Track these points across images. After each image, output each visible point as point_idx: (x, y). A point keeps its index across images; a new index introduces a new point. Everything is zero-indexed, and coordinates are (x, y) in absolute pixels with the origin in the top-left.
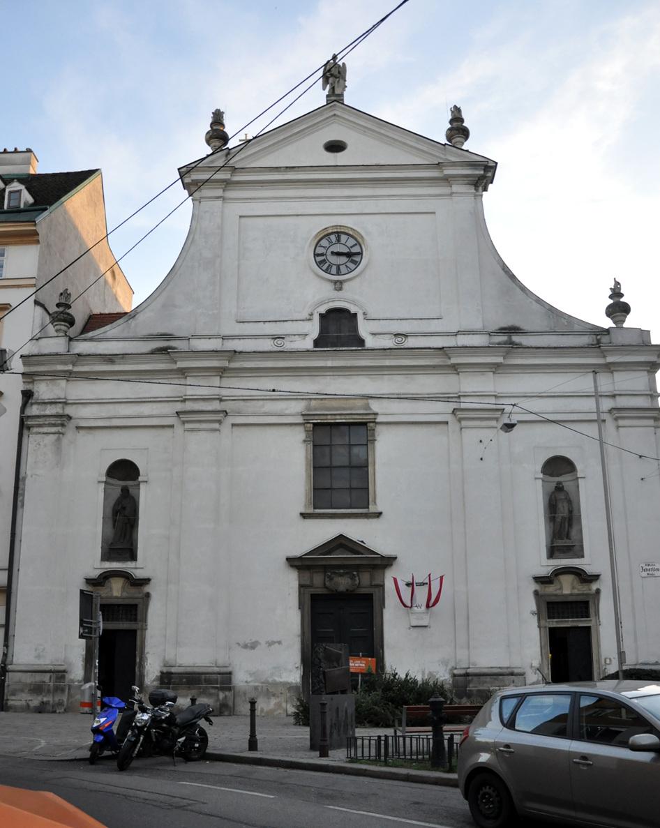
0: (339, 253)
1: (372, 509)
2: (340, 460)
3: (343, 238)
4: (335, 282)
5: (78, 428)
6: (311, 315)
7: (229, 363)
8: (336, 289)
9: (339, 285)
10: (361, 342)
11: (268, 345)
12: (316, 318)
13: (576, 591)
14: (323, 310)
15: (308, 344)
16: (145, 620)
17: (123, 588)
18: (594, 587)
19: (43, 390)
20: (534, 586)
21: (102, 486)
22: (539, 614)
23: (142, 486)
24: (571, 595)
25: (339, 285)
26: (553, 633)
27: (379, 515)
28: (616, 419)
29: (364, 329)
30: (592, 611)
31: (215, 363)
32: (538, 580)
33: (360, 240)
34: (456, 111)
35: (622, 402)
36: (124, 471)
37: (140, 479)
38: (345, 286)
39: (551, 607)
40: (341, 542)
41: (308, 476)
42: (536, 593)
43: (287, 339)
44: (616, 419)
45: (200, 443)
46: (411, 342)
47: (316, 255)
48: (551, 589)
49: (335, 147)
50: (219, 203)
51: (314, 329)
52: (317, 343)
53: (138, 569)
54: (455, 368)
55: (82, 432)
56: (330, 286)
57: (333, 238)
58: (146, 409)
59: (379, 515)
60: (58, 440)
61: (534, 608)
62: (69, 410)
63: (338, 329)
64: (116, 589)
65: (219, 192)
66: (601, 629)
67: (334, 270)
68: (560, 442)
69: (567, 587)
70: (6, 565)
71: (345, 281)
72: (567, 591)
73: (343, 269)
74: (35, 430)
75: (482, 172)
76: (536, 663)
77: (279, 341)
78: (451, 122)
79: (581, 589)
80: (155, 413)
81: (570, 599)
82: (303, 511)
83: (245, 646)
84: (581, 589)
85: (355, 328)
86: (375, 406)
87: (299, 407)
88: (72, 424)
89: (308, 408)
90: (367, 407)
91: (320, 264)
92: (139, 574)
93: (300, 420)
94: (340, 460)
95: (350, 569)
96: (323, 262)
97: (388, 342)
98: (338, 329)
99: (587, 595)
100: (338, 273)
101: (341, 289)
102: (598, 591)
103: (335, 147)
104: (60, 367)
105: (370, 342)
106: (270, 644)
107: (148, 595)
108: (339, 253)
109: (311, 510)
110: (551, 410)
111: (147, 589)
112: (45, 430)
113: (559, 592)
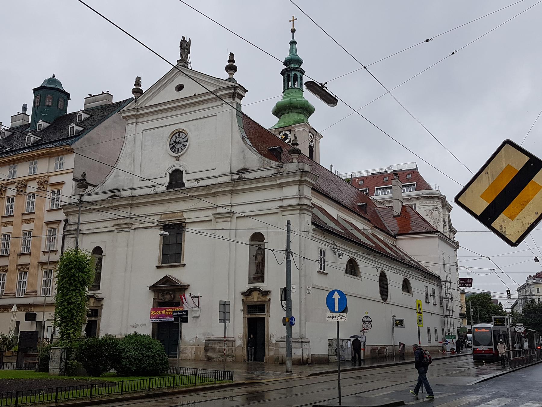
0: (178, 143)
1: (182, 263)
3: (181, 134)
4: (176, 157)
5: (83, 234)
7: (133, 202)
8: (177, 160)
9: (177, 158)
10: (184, 185)
11: (149, 191)
12: (168, 175)
13: (260, 300)
14: (170, 171)
15: (164, 189)
17: (94, 303)
19: (73, 219)
20: (242, 297)
22: (243, 310)
24: (258, 301)
25: (177, 158)
27: (184, 265)
29: (185, 178)
30: (266, 309)
31: (126, 202)
32: (242, 293)
34: (232, 55)
37: (103, 254)
38: (180, 158)
39: (250, 308)
40: (166, 280)
41: (160, 249)
42: (243, 300)
43: (157, 187)
45: (122, 237)
46: (202, 183)
47: (170, 145)
48: (249, 299)
49: (180, 88)
50: (134, 125)
51: (166, 181)
52: (168, 187)
54: (215, 194)
55: (85, 236)
56: (175, 159)
57: (177, 135)
59: (184, 265)
63: (176, 179)
65: (134, 120)
66: (270, 319)
67: (176, 152)
68: (256, 225)
69: (255, 298)
71: (180, 156)
72: (256, 300)
73: (180, 150)
74: (68, 236)
75: (233, 91)
76: (241, 336)
77: (152, 189)
78: (229, 61)
79: (262, 298)
80: (108, 225)
81: (258, 303)
82: (157, 265)
84: (262, 298)
86: (185, 216)
88: (81, 232)
89: (161, 219)
91: (171, 149)
92: (100, 296)
95: (174, 291)
96: (173, 147)
97: (193, 184)
98: (176, 179)
99: (265, 301)
100: (178, 152)
101: (179, 160)
102: (270, 300)
103: (180, 88)
104: (75, 209)
105: (187, 185)
106: (142, 325)
107: (102, 305)
108: (178, 143)
109: (160, 265)
110: (254, 209)
112: (71, 236)
113: (252, 300)
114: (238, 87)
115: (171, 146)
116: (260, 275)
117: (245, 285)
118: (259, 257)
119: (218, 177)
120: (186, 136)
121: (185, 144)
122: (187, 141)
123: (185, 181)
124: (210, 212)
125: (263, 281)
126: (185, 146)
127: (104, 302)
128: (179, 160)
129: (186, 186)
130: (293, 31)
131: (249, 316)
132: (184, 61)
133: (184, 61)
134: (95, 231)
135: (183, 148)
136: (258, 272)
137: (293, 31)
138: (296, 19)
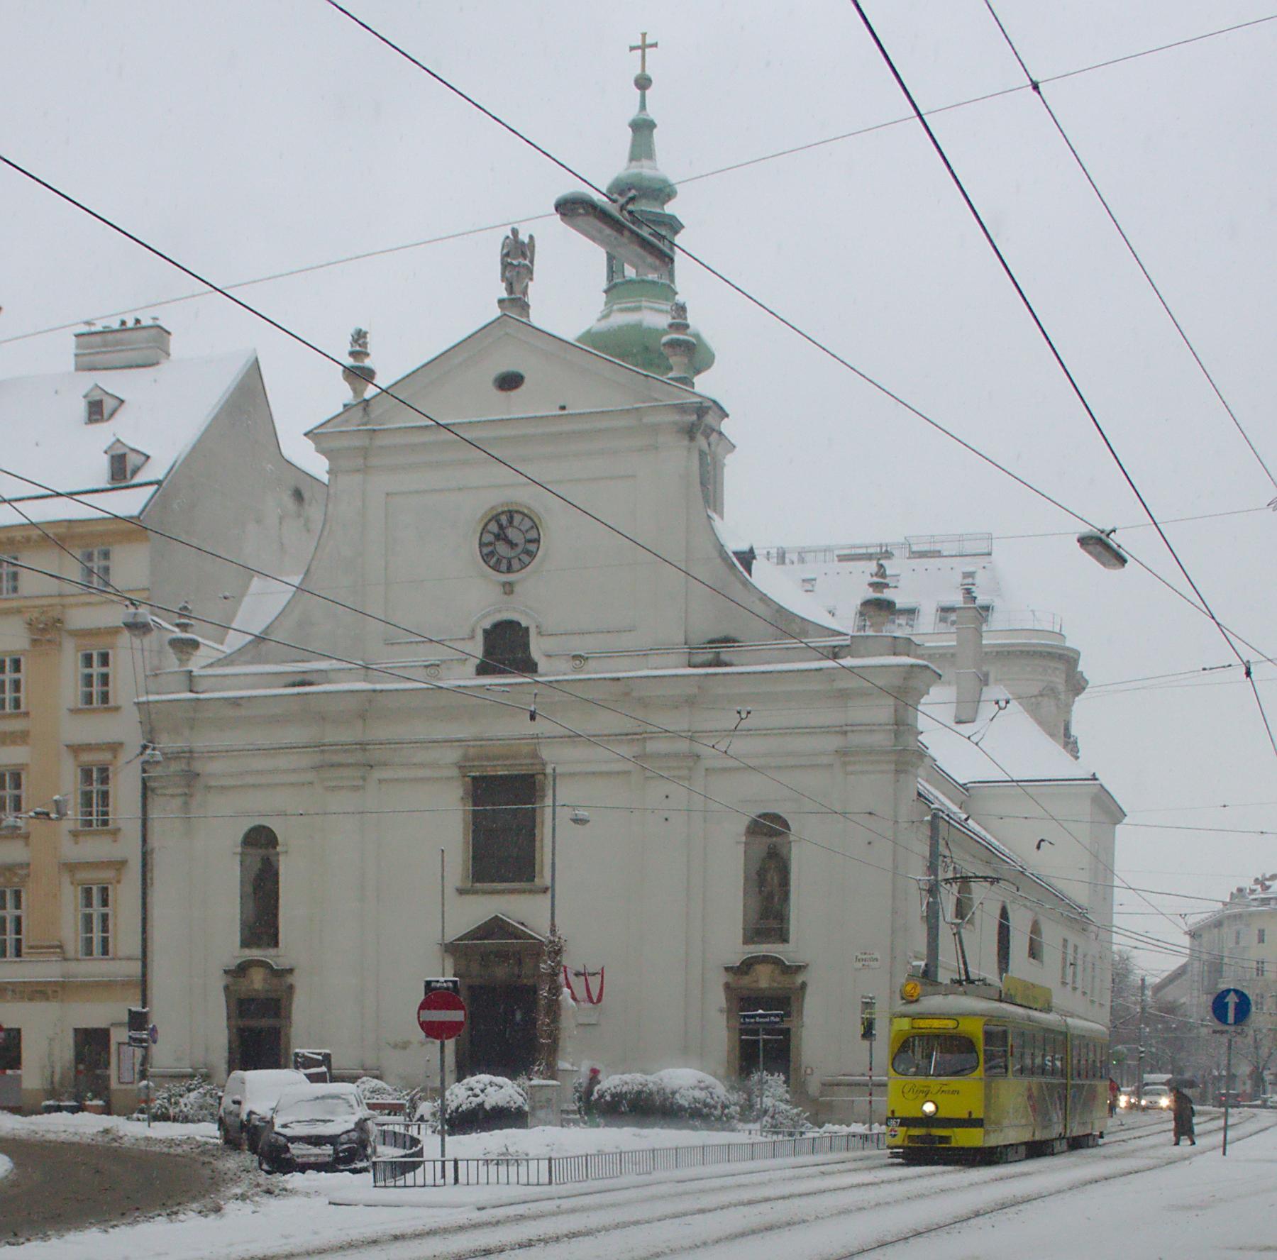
0: (507, 540)
2: (505, 821)
3: (517, 518)
6: (473, 631)
9: (508, 588)
10: (529, 666)
14: (487, 624)
16: (289, 1017)
17: (265, 980)
18: (799, 979)
21: (238, 858)
23: (282, 858)
25: (508, 588)
26: (241, 1031)
28: (845, 764)
32: (727, 969)
33: (536, 520)
35: (855, 740)
36: (261, 841)
37: (279, 849)
38: (517, 588)
40: (496, 927)
42: (727, 986)
44: (845, 764)
47: (481, 545)
48: (746, 981)
49: (509, 382)
51: (477, 648)
52: (482, 670)
53: (277, 957)
56: (500, 590)
57: (504, 519)
58: (283, 762)
60: (186, 803)
61: (724, 1004)
62: (198, 766)
63: (506, 648)
64: (257, 980)
66: (805, 1033)
67: (504, 566)
69: (764, 979)
70: (138, 952)
72: (764, 984)
82: (459, 884)
83: (395, 1046)
85: (526, 647)
87: (453, 755)
89: (466, 758)
90: (535, 755)
91: (486, 558)
93: (455, 772)
94: (505, 821)
96: (492, 554)
98: (506, 648)
100: (509, 570)
102: (804, 986)
103: (509, 382)
105: (543, 665)
107: (291, 987)
108: (507, 540)
111: (290, 979)
114: (709, 408)
115: (486, 550)
116: (774, 924)
117: (734, 949)
118: (773, 877)
119: (644, 654)
120: (535, 526)
121: (532, 547)
122: (537, 541)
123: (535, 653)
124: (626, 750)
125: (785, 939)
126: (532, 555)
127: (296, 980)
128: (512, 592)
129: (540, 668)
130: (643, 83)
131: (241, 1023)
132: (515, 302)
133: (515, 302)
134: (250, 780)
135: (525, 558)
136: (769, 909)
137: (643, 83)
138: (655, 45)
